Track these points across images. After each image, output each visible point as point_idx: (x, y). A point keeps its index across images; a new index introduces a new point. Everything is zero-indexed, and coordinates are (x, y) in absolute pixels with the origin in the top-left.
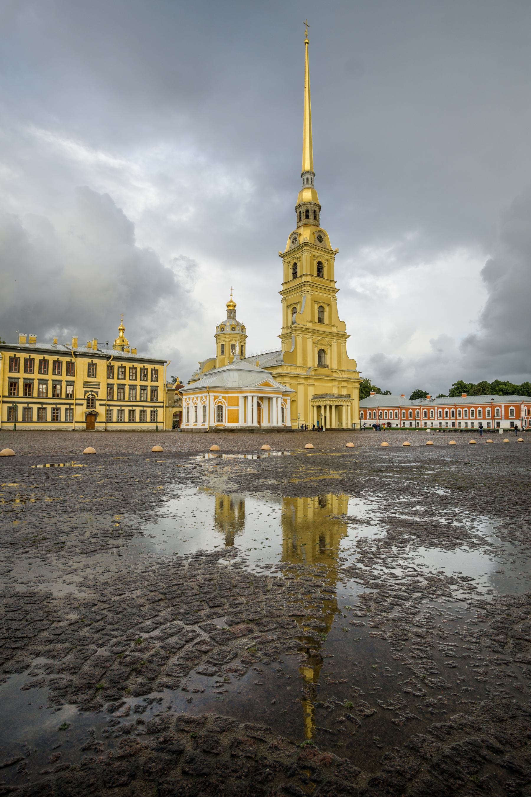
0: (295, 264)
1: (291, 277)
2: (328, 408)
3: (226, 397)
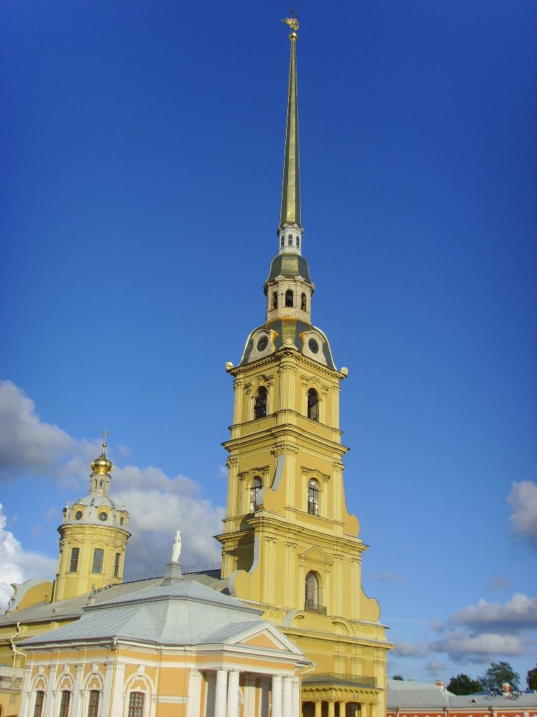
0: (263, 392)
1: (251, 416)
2: (332, 708)
3: (156, 668)
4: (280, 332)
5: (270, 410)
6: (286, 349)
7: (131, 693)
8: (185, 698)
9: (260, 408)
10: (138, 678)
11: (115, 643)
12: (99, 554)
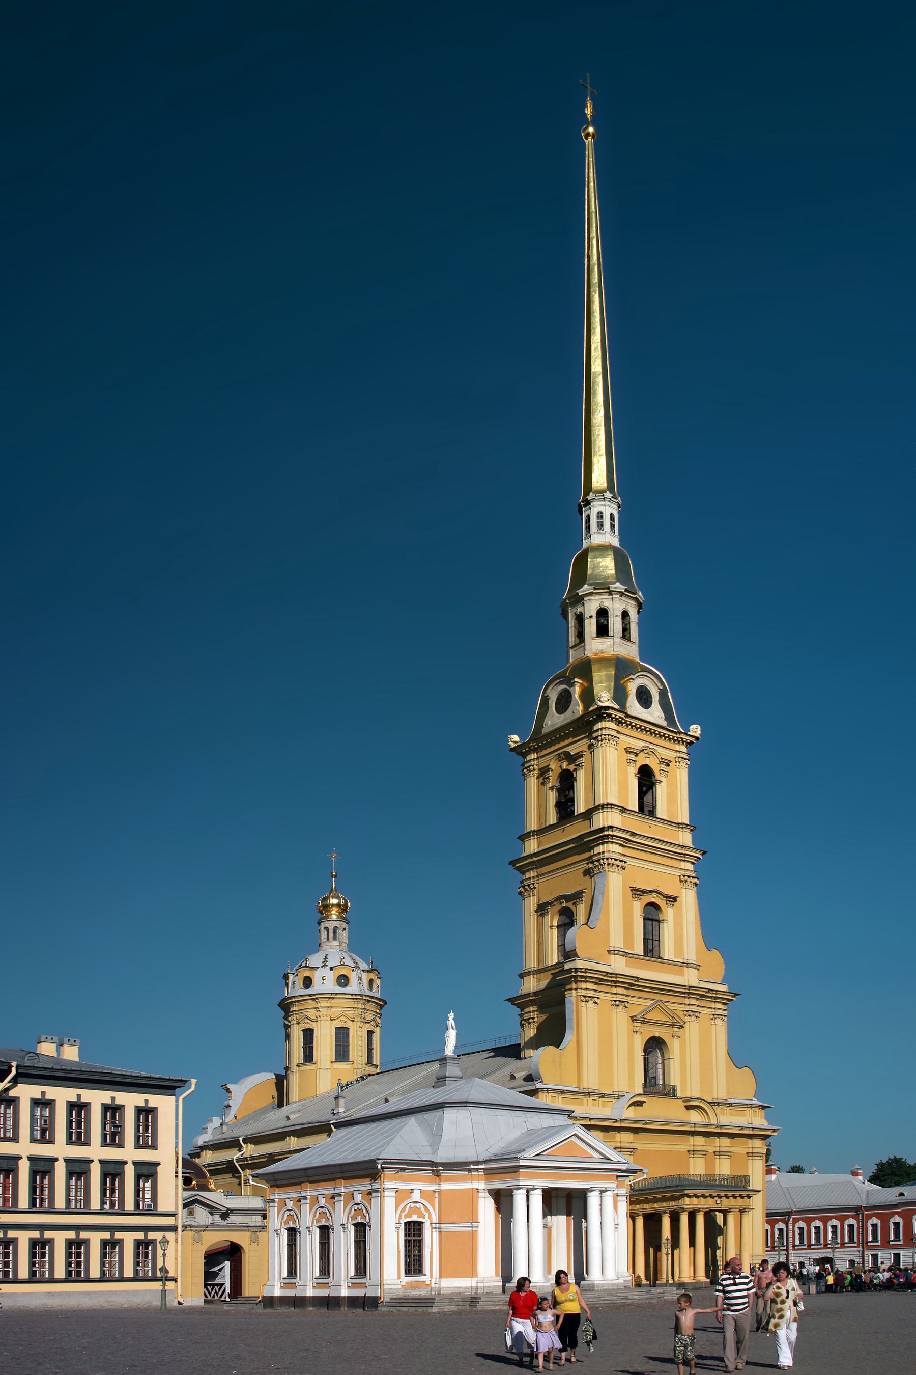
4: (590, 681)
5: (581, 807)
6: (601, 708)
7: (405, 1223)
8: (474, 1224)
10: (413, 1205)
11: (379, 1167)
12: (342, 1035)
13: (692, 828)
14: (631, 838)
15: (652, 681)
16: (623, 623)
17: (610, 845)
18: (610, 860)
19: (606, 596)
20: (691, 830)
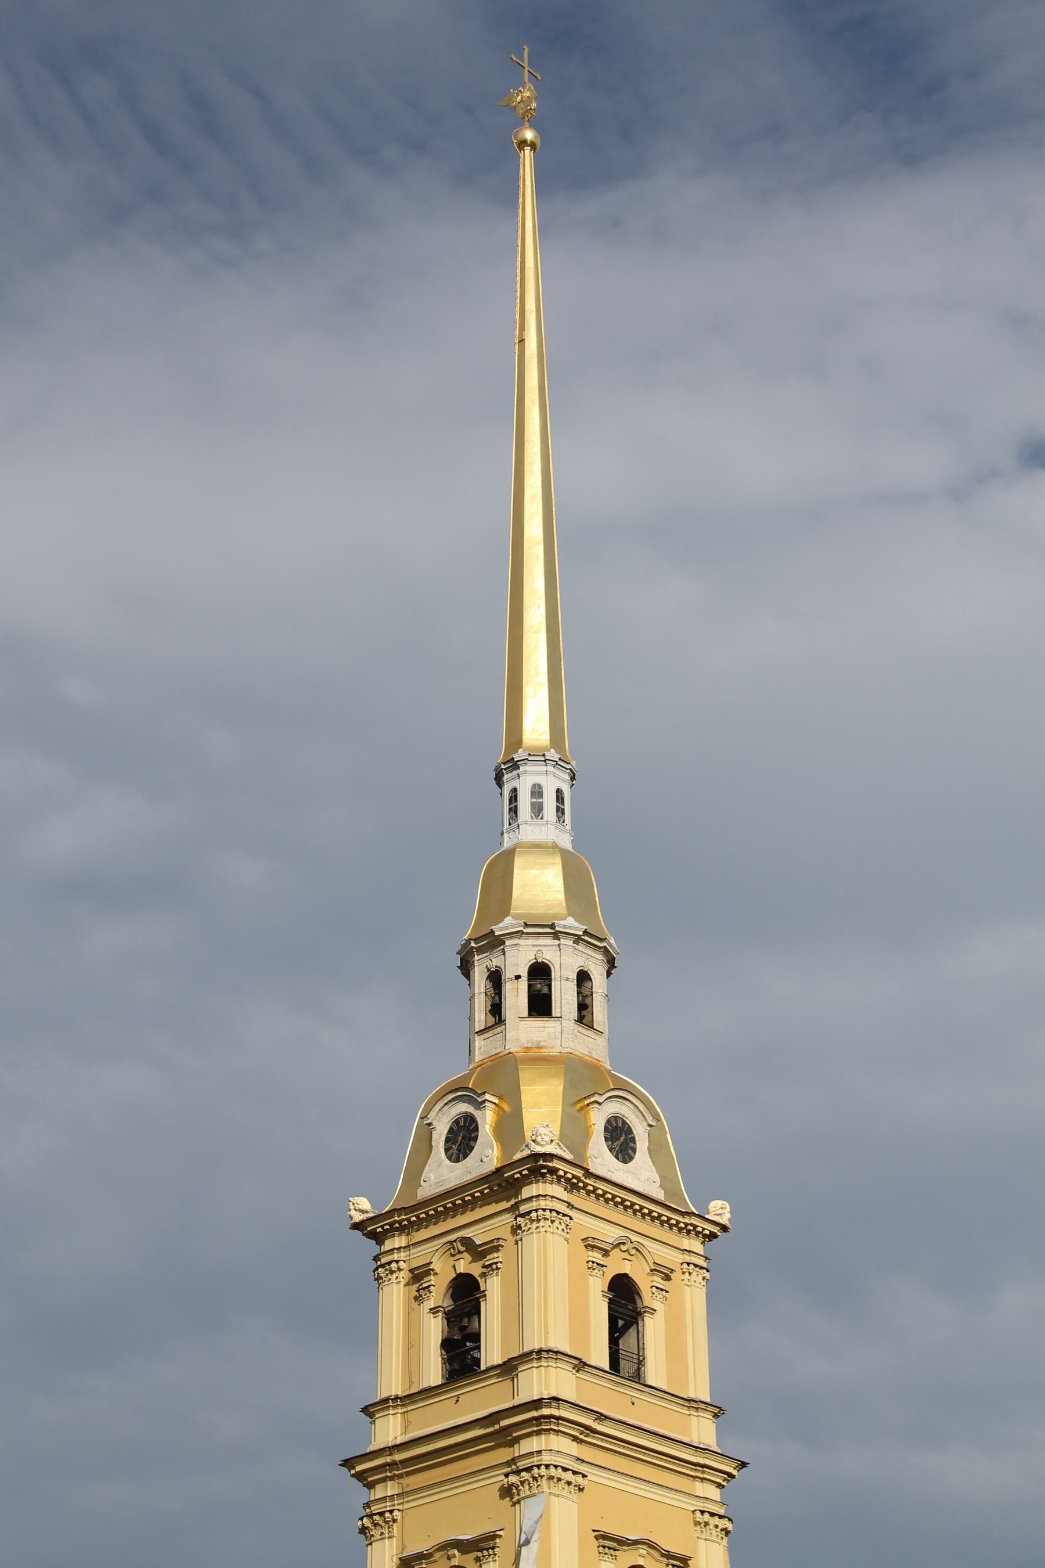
1: (433, 1373)
6: (536, 1156)
9: (461, 1343)
13: (716, 1410)
14: (595, 1425)
15: (635, 1110)
16: (579, 993)
17: (553, 1437)
18: (552, 1468)
19: (549, 941)
20: (716, 1416)
